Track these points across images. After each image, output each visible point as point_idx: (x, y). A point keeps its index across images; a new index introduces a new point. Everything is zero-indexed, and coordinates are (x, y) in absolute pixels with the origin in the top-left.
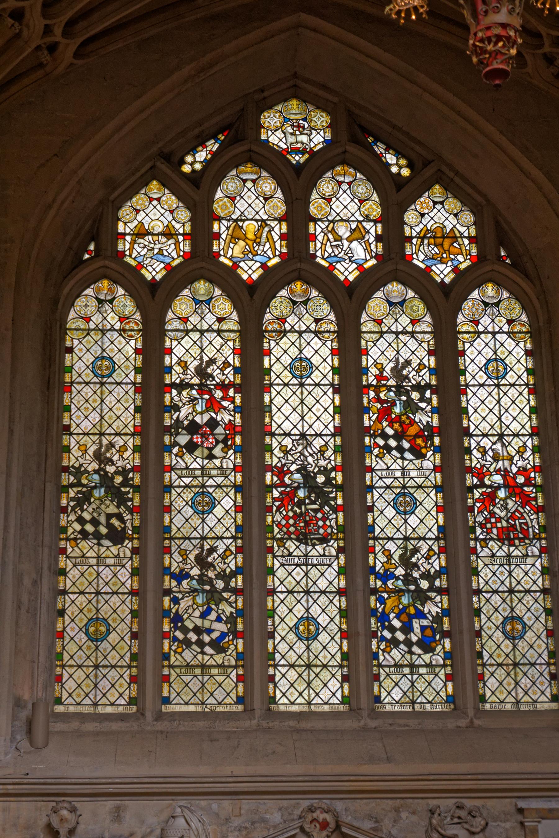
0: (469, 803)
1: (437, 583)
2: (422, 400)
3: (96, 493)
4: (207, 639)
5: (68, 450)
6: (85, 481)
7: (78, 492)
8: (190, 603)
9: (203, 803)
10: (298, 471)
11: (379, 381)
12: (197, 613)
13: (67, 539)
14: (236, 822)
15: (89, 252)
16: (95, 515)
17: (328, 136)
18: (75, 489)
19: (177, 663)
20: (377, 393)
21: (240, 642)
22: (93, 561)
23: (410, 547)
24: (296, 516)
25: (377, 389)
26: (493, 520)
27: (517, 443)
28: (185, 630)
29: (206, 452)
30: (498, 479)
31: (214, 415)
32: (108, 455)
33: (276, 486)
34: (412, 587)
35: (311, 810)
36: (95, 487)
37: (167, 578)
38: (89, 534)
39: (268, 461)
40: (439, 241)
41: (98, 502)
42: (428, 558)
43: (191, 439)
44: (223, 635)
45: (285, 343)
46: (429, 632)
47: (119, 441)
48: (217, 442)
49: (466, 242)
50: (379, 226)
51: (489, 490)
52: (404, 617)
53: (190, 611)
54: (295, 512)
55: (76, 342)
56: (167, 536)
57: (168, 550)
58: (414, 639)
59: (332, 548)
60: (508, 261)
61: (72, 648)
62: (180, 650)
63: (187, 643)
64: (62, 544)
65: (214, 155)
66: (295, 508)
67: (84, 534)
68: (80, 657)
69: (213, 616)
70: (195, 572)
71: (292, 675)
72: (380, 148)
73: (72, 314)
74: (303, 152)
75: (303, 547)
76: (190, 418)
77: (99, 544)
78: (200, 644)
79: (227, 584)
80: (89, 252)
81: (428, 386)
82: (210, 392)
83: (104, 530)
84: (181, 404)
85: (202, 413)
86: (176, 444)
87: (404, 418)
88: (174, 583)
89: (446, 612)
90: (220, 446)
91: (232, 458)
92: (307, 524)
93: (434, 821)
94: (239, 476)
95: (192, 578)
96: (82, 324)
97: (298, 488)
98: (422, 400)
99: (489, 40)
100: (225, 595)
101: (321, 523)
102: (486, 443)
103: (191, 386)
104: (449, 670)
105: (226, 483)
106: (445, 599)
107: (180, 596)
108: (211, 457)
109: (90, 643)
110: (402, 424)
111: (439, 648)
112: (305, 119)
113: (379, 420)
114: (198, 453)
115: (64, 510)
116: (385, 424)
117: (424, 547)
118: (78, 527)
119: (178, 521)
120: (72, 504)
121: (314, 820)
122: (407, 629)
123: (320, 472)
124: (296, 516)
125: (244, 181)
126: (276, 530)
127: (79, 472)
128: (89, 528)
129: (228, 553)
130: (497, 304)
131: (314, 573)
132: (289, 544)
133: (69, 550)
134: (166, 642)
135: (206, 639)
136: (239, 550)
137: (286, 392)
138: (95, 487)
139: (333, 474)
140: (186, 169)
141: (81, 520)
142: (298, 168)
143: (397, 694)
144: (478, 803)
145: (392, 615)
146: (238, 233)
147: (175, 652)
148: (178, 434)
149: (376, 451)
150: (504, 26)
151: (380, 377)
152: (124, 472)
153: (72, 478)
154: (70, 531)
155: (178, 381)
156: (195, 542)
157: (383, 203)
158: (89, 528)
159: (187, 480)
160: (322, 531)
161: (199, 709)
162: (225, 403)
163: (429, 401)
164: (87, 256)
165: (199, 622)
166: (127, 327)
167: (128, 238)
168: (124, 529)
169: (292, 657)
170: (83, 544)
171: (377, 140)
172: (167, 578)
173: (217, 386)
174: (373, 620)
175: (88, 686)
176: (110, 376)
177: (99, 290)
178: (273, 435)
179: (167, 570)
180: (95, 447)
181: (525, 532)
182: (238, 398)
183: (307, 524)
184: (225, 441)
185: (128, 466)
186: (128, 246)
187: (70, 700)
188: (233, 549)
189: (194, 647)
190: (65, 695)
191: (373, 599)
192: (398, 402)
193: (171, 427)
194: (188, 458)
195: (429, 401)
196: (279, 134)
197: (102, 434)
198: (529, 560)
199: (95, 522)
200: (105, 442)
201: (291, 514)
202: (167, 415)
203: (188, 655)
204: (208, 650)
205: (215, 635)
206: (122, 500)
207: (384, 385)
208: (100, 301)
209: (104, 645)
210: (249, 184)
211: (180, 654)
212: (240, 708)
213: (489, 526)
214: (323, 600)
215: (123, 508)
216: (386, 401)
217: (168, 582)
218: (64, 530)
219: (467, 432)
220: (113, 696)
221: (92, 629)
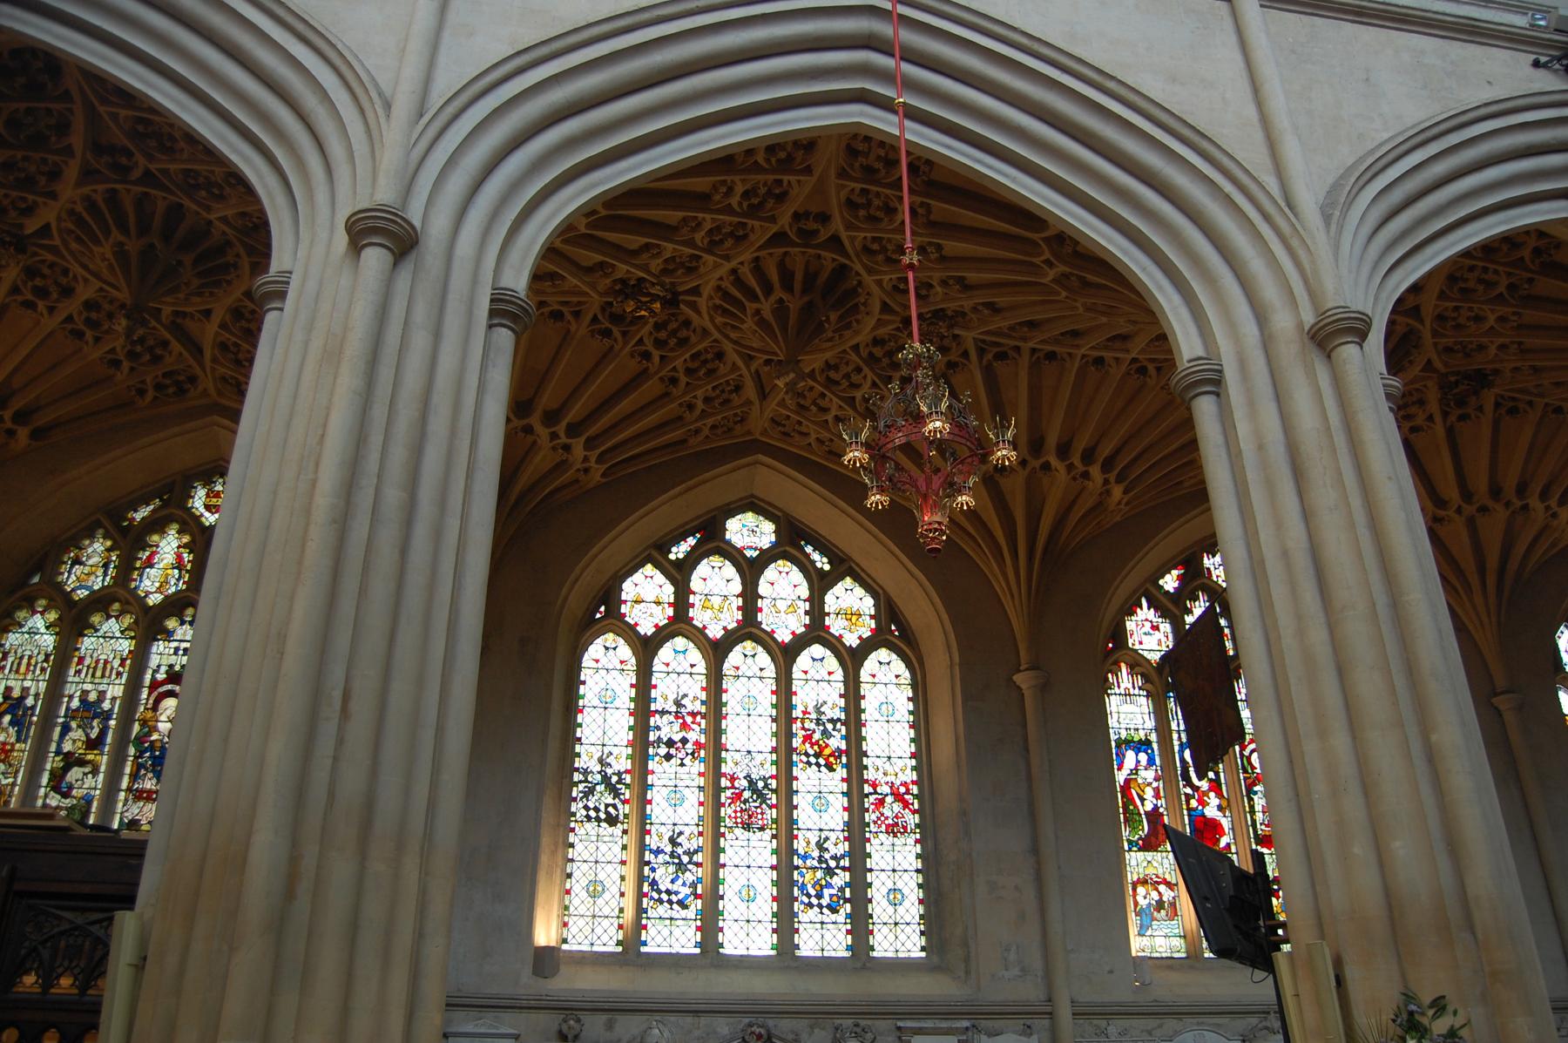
0: (863, 1023)
1: (842, 863)
2: (834, 729)
3: (598, 787)
4: (674, 898)
9: (672, 1019)
10: (745, 778)
13: (576, 821)
14: (697, 1033)
15: (601, 613)
16: (597, 804)
17: (773, 539)
20: (803, 723)
22: (594, 838)
23: (823, 836)
24: (742, 811)
26: (883, 818)
27: (900, 763)
28: (659, 892)
29: (679, 762)
30: (886, 789)
33: (728, 788)
34: (824, 866)
35: (750, 1025)
36: (598, 784)
39: (723, 770)
40: (848, 617)
42: (836, 844)
44: (687, 896)
45: (738, 683)
46: (835, 899)
48: (687, 754)
49: (868, 618)
50: (807, 603)
51: (880, 797)
52: (818, 887)
53: (664, 877)
55: (588, 677)
58: (825, 904)
59: (768, 834)
60: (896, 633)
61: (576, 902)
63: (661, 901)
64: (572, 825)
65: (693, 548)
66: (742, 805)
67: (589, 818)
68: (583, 909)
69: (680, 882)
70: (668, 849)
72: (809, 549)
73: (586, 657)
74: (756, 549)
76: (668, 736)
77: (599, 826)
78: (670, 902)
79: (691, 859)
80: (601, 613)
81: (839, 720)
82: (683, 718)
83: (603, 816)
84: (661, 726)
86: (657, 754)
87: (821, 742)
88: (652, 856)
89: (847, 885)
90: (690, 757)
92: (750, 817)
93: (838, 1035)
96: (594, 665)
98: (834, 729)
99: (931, 531)
100: (690, 867)
101: (760, 816)
102: (879, 762)
103: (670, 713)
104: (849, 927)
105: (694, 784)
106: (847, 874)
107: (656, 866)
108: (682, 765)
110: (820, 746)
111: (842, 911)
112: (757, 526)
113: (804, 742)
114: (673, 760)
115: (575, 799)
116: (808, 745)
117: (833, 836)
120: (581, 795)
121: (753, 1033)
122: (819, 896)
123: (760, 779)
124: (742, 811)
125: (713, 567)
126: (727, 820)
127: (586, 772)
128: (593, 814)
130: (888, 664)
132: (736, 830)
133: (577, 829)
135: (674, 898)
136: (700, 834)
138: (598, 784)
139: (769, 781)
140: (672, 557)
141: (586, 808)
142: (751, 561)
143: (811, 943)
144: (869, 1022)
145: (809, 886)
146: (708, 604)
148: (659, 747)
150: (939, 523)
151: (804, 713)
152: (619, 774)
153: (581, 776)
154: (578, 815)
157: (811, 588)
158: (593, 814)
160: (760, 822)
162: (694, 726)
163: (839, 731)
164: (598, 616)
165: (670, 886)
166: (625, 668)
167: (629, 604)
168: (617, 815)
170: (588, 825)
171: (807, 544)
173: (689, 714)
174: (796, 888)
175: (587, 930)
177: (606, 640)
178: (727, 750)
181: (905, 828)
182: (703, 722)
183: (750, 817)
184: (693, 754)
186: (628, 609)
187: (574, 941)
188: (696, 834)
189: (665, 904)
190: (570, 937)
191: (796, 872)
195: (839, 731)
196: (739, 535)
198: (908, 848)
199: (597, 809)
200: (606, 751)
201: (739, 809)
202: (651, 734)
206: (616, 793)
208: (607, 648)
210: (716, 569)
213: (879, 822)
215: (617, 801)
216: (809, 730)
218: (574, 814)
219: (865, 754)
220: (605, 938)
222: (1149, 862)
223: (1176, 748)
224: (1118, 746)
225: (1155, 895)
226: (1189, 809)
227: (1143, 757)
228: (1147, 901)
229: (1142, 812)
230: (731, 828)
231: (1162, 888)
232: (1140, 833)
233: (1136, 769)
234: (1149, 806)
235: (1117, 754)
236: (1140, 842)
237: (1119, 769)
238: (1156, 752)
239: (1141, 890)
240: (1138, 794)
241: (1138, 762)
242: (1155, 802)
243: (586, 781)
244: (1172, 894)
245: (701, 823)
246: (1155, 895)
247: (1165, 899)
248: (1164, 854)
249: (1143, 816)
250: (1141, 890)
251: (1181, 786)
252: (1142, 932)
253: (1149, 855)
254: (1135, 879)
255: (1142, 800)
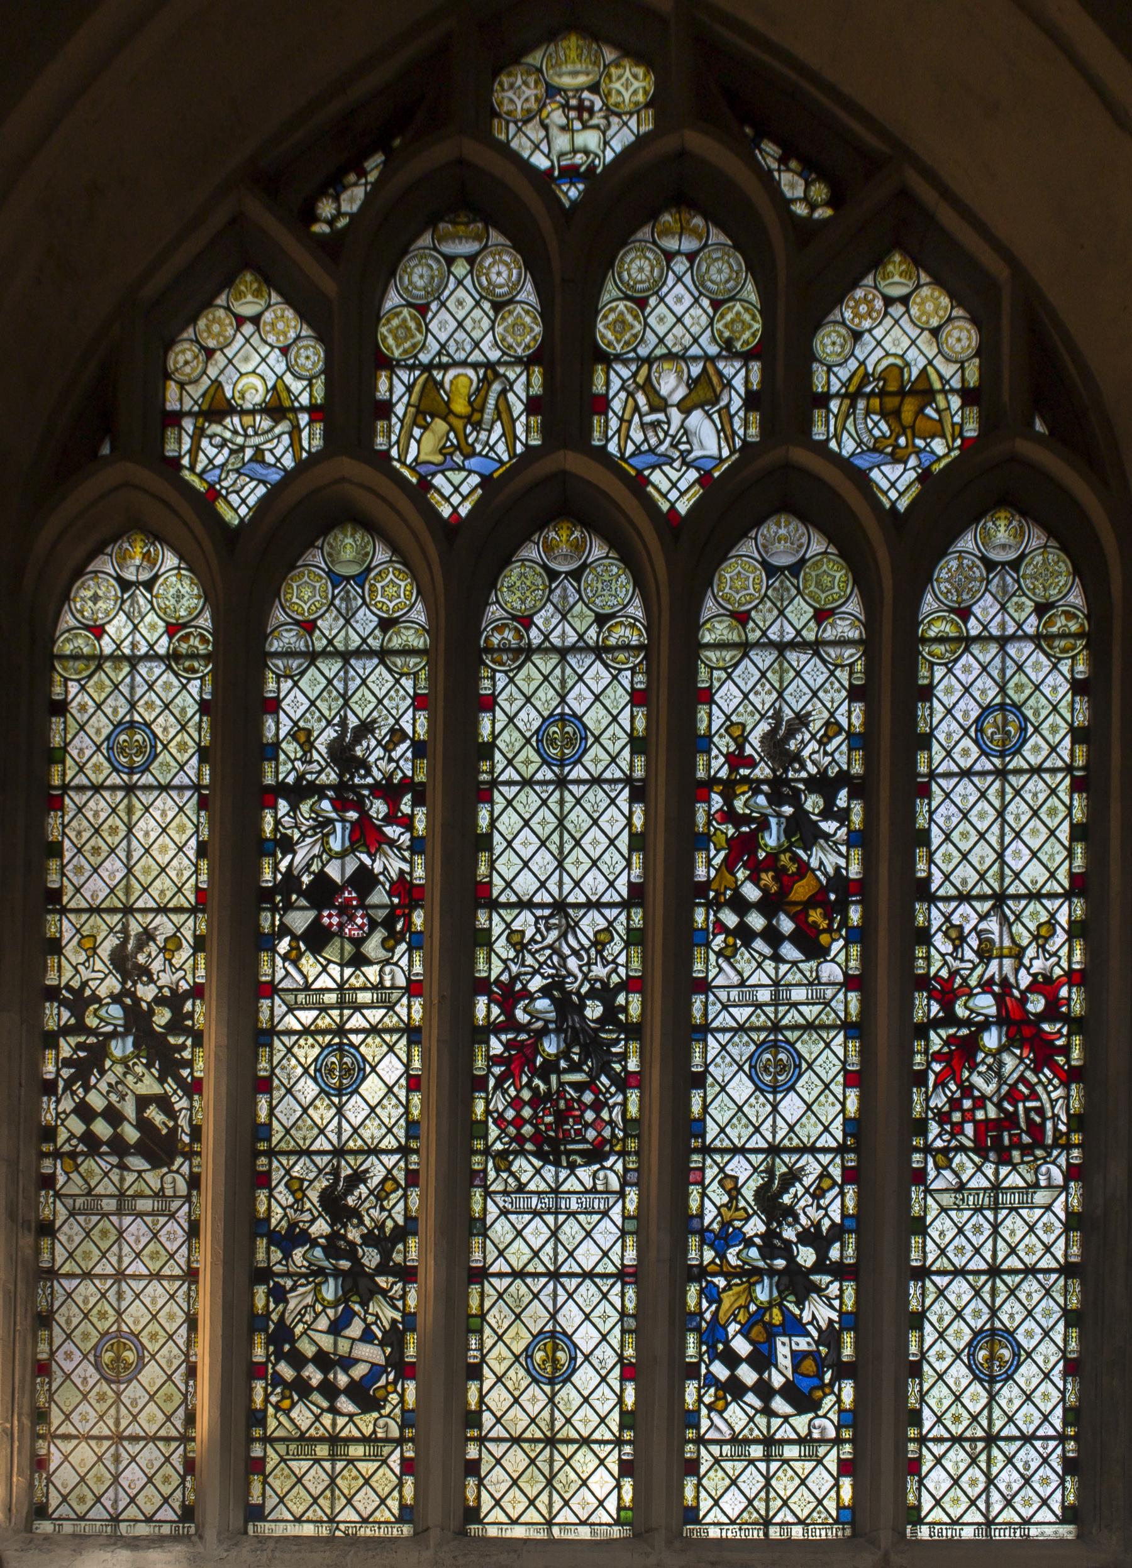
5: (55, 947)
6: (91, 1022)
7: (80, 1046)
8: (309, 1300)
10: (545, 991)
11: (733, 769)
12: (323, 1323)
13: (57, 1154)
16: (113, 1098)
18: (73, 1040)
19: (280, 1433)
21: (411, 1386)
22: (110, 1205)
24: (537, 1100)
25: (729, 790)
28: (297, 1360)
31: (367, 861)
32: (141, 959)
33: (496, 1029)
36: (114, 1035)
37: (261, 1243)
38: (101, 1143)
41: (119, 1069)
43: (318, 919)
44: (376, 1371)
47: (164, 926)
48: (373, 925)
54: (535, 1090)
56: (263, 1146)
57: (264, 1180)
62: (286, 1404)
63: (302, 1388)
64: (47, 1167)
66: (537, 1081)
69: (355, 1329)
70: (321, 1227)
71: (516, 1460)
75: (549, 1172)
76: (315, 868)
77: (123, 1167)
78: (329, 1390)
83: (131, 1134)
85: (342, 855)
86: (285, 930)
88: (276, 1255)
91: (404, 962)
92: (561, 1117)
94: (417, 1005)
95: (314, 1243)
97: (544, 1032)
100: (382, 1281)
101: (589, 1116)
103: (319, 791)
109: (105, 1387)
110: (780, 874)
113: (729, 865)
115: (49, 1087)
116: (741, 874)
118: (76, 1125)
119: (288, 1111)
120: (66, 1073)
123: (592, 994)
126: (494, 1131)
128: (102, 1129)
129: (389, 1186)
131: (571, 1230)
133: (61, 1179)
134: (259, 1386)
137: (529, 800)
138: (114, 1035)
141: (84, 1112)
147: (277, 1408)
148: (289, 906)
149: (718, 942)
151: (736, 760)
152: (173, 1000)
154: (63, 1135)
155: (290, 779)
156: (322, 1161)
158: (102, 1129)
159: (307, 1017)
161: (324, 1531)
162: (392, 831)
165: (326, 1342)
168: (173, 1131)
169: (517, 1421)
172: (261, 1243)
173: (378, 790)
176: (145, 769)
179: (260, 1226)
180: (113, 942)
183: (561, 1117)
184: (388, 923)
185: (184, 986)
189: (316, 1397)
192: (773, 821)
193: (275, 889)
194: (308, 963)
197: (128, 910)
200: (135, 928)
203: (302, 1415)
204: (345, 1404)
205: (359, 1371)
207: (746, 780)
209: (132, 1392)
211: (287, 1412)
212: (406, 1530)
214: (588, 1292)
216: (746, 819)
217: (266, 1254)
218: (50, 1133)
221: (108, 1357)
230: (503, 1154)
243: (80, 1028)
245: (413, 1145)
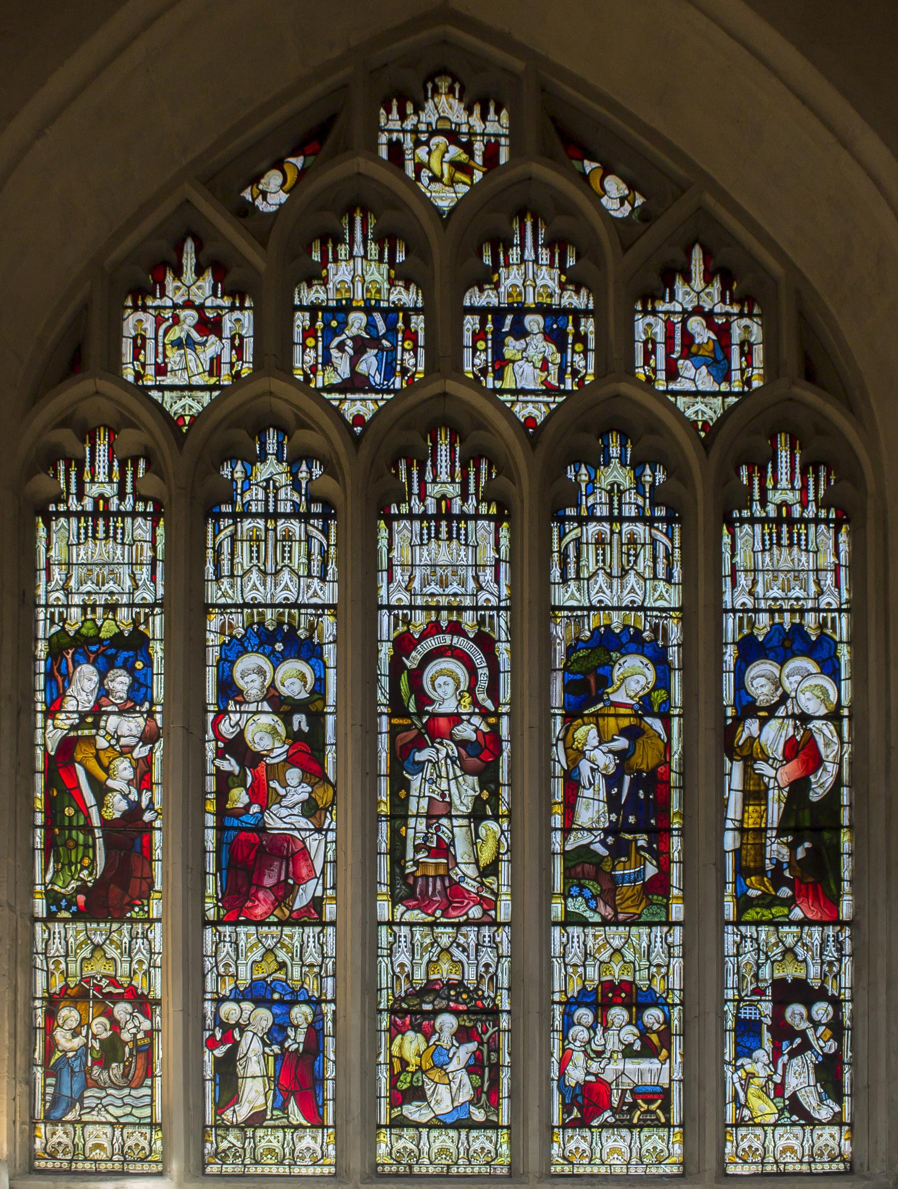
222: (97, 947)
223: (213, 655)
224: (56, 651)
225: (100, 1026)
226: (222, 812)
227: (120, 682)
228: (78, 1042)
229: (96, 822)
231: (122, 1010)
232: (84, 874)
233: (97, 712)
234: (117, 806)
235: (49, 675)
236: (81, 898)
237: (51, 713)
238: (158, 666)
239: (69, 1015)
240: (90, 776)
241: (104, 693)
242: (134, 796)
244: (146, 1025)
246: (100, 1026)
247: (126, 1036)
248: (139, 927)
249: (98, 833)
250: (69, 1015)
251: (210, 755)
252: (57, 1114)
253: (98, 931)
254: (57, 984)
255: (101, 791)
